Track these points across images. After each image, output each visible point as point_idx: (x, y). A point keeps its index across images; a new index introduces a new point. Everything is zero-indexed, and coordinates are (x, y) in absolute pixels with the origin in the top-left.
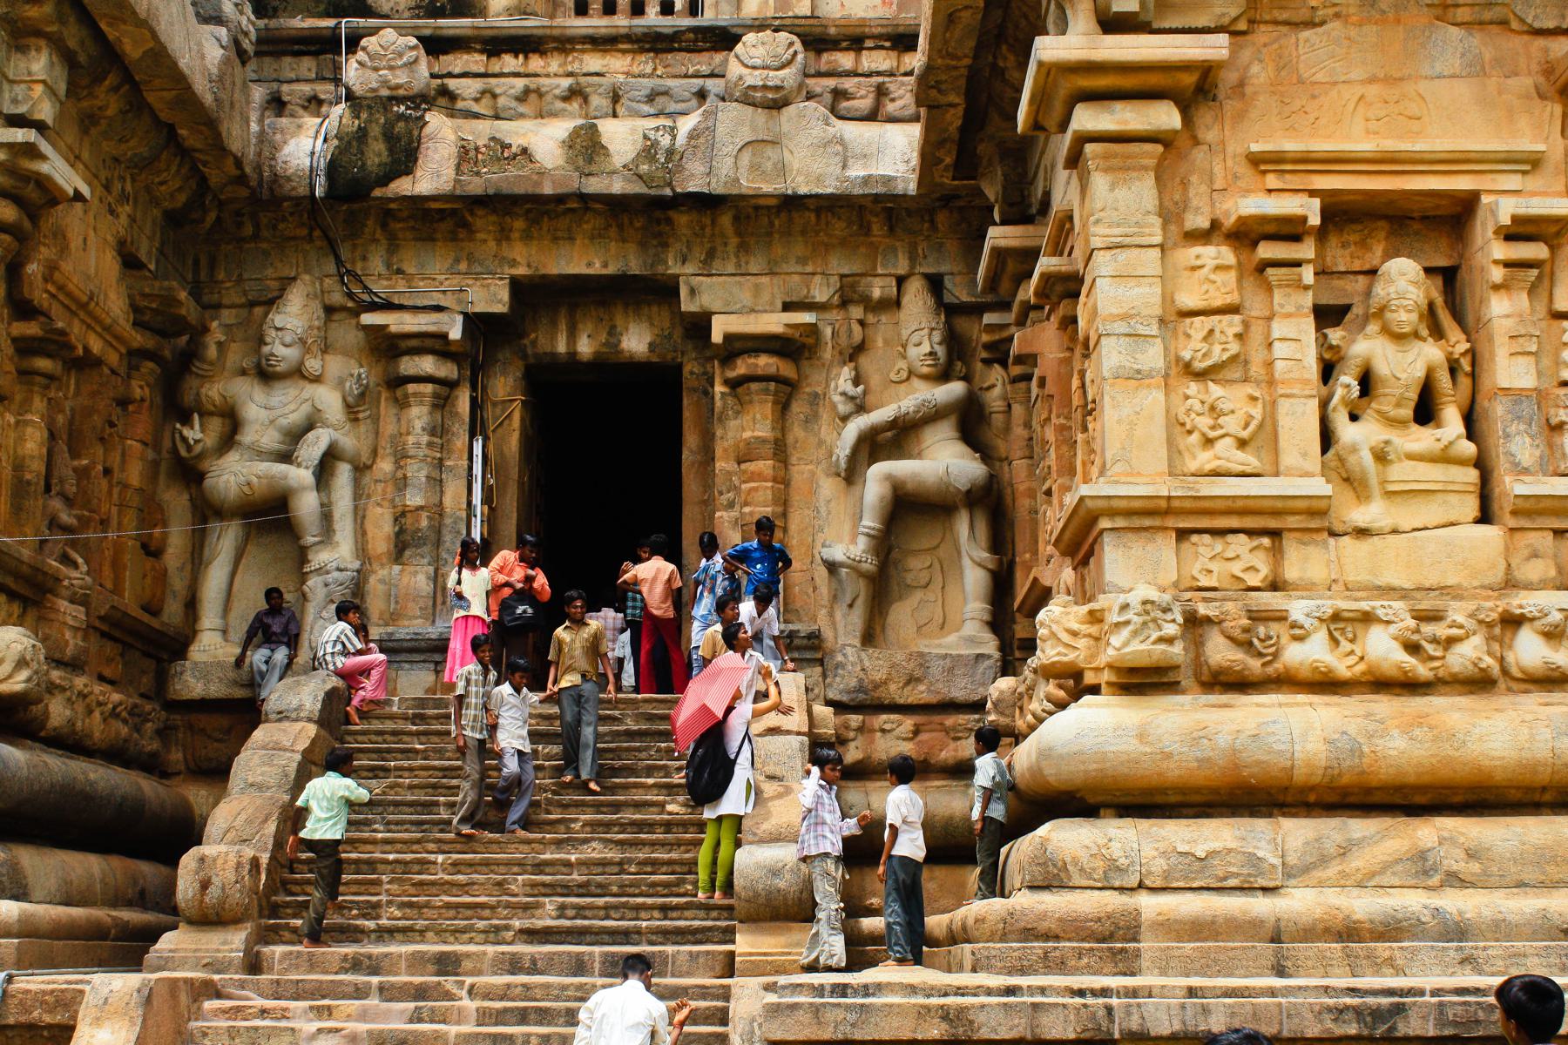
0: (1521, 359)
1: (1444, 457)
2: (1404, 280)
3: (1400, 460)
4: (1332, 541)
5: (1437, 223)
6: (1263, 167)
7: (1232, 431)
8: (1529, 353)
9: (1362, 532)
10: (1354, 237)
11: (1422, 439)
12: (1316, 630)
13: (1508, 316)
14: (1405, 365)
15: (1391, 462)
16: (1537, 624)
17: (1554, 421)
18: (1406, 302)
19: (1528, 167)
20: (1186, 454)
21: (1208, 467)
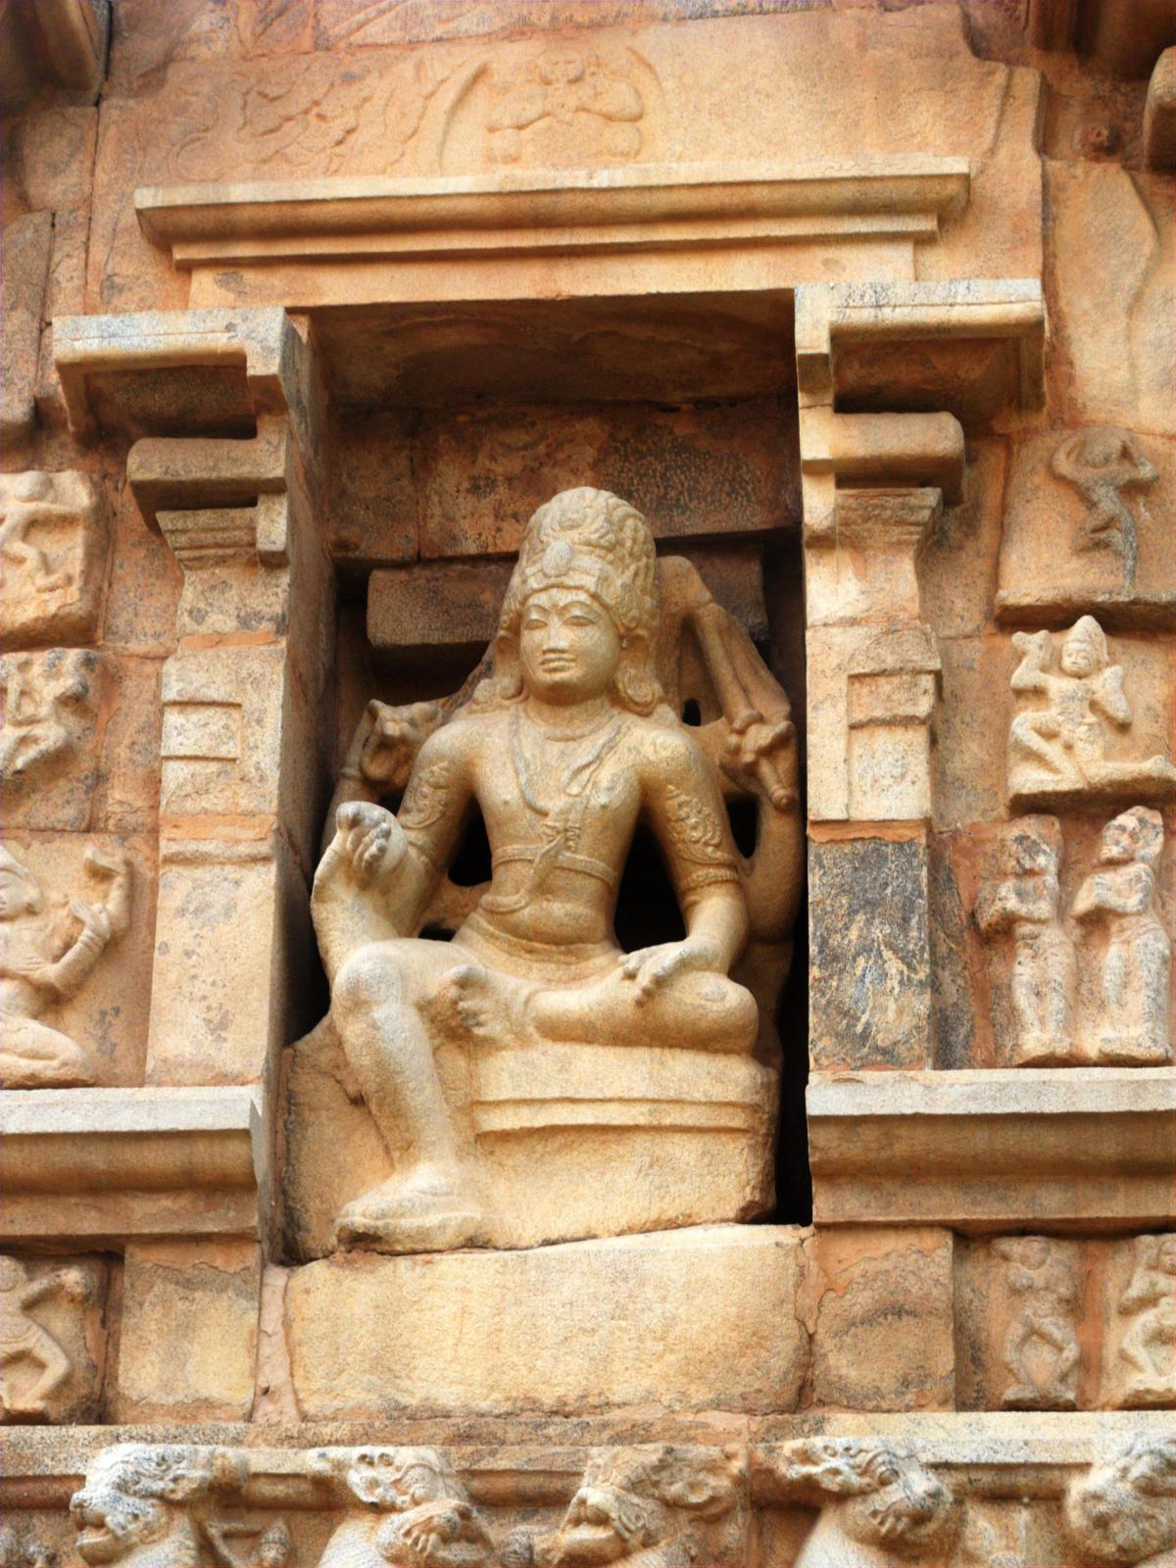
0: (883, 739)
1: (649, 1028)
2: (577, 548)
3: (523, 1040)
4: (277, 1277)
5: (683, 390)
6: (179, 254)
8: (908, 721)
9: (366, 1244)
11: (609, 982)
12: (151, 1534)
13: (853, 622)
15: (490, 1045)
16: (856, 1509)
17: (988, 916)
18: (563, 598)
19: (927, 224)
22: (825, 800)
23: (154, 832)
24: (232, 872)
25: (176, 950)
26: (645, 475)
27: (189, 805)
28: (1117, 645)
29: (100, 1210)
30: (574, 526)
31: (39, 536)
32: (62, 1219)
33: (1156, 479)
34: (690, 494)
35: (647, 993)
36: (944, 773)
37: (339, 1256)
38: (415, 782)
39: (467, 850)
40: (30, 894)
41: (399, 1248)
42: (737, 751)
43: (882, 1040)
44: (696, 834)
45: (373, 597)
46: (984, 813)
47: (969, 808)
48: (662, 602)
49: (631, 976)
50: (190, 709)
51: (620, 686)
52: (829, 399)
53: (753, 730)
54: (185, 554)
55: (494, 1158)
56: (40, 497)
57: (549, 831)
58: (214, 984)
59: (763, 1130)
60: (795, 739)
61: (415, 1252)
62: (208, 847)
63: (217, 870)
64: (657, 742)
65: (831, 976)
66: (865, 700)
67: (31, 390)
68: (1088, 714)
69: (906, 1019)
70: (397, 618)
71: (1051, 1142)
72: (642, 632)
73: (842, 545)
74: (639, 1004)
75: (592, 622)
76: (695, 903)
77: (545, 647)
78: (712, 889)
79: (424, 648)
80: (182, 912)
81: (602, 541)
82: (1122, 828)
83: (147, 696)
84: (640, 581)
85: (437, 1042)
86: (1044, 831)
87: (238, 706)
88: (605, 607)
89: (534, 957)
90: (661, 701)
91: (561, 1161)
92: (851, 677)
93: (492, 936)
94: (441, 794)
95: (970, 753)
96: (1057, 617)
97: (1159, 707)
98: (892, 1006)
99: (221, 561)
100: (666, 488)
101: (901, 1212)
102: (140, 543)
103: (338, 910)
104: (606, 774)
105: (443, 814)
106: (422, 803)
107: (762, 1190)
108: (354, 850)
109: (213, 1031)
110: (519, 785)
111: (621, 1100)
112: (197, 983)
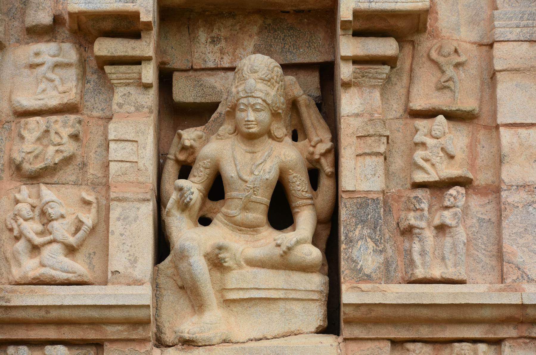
0: (368, 160)
1: (284, 263)
3: (240, 266)
7: (59, 237)
8: (378, 154)
13: (357, 115)
14: (254, 165)
20: (12, 262)
21: (32, 274)
22: (348, 181)
23: (107, 186)
24: (137, 205)
25: (117, 233)
26: (277, 39)
27: (120, 179)
28: (451, 124)
29: (95, 330)
31: (57, 70)
32: (82, 333)
33: (466, 61)
34: (293, 47)
35: (285, 252)
36: (388, 171)
37: (179, 347)
39: (216, 190)
40: (63, 211)
41: (200, 344)
42: (312, 154)
43: (367, 271)
44: (299, 188)
45: (174, 82)
46: (402, 186)
47: (397, 184)
50: (118, 142)
51: (272, 132)
52: (351, 32)
53: (319, 145)
54: (115, 82)
55: (229, 308)
56: (58, 55)
57: (247, 188)
58: (131, 246)
59: (324, 300)
60: (335, 152)
61: (205, 346)
62: (128, 195)
63: (131, 203)
65: (349, 248)
66: (362, 145)
67: (52, 12)
68: (441, 153)
69: (375, 264)
70: (184, 91)
71: (426, 313)
72: (280, 111)
73: (354, 85)
75: (263, 110)
76: (298, 212)
77: (246, 119)
78: (305, 207)
79: (194, 103)
80: (118, 219)
81: (266, 78)
82: (451, 195)
83: (101, 133)
85: (210, 267)
86: (424, 195)
87: (137, 141)
88: (268, 104)
89: (241, 232)
90: (286, 135)
91: (253, 310)
92: (357, 137)
93: (226, 224)
95: (398, 163)
96: (430, 114)
97: (465, 147)
98: (370, 259)
99: (128, 85)
100: (285, 44)
101: (373, 335)
102: (95, 72)
103: (175, 220)
104: (267, 166)
105: (208, 178)
106: (200, 174)
107: (323, 321)
108: (181, 199)
109: (131, 264)
110: (237, 170)
111: (275, 289)
112: (125, 246)
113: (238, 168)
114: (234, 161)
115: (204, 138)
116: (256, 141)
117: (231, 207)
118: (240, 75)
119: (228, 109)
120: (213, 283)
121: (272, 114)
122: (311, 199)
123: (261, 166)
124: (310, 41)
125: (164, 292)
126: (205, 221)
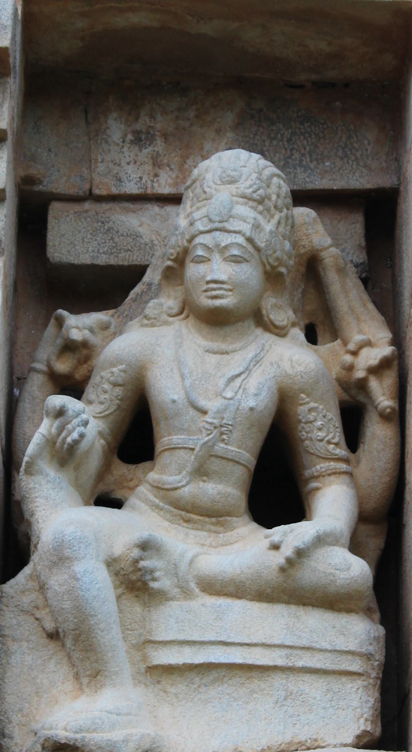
10: (161, 123)
18: (225, 239)
26: (275, 139)
30: (233, 182)
34: (311, 156)
35: (289, 561)
38: (95, 379)
39: (136, 436)
42: (350, 368)
44: (321, 434)
45: (52, 222)
48: (295, 245)
49: (276, 547)
51: (264, 312)
53: (365, 352)
55: (159, 686)
57: (207, 426)
59: (374, 675)
64: (292, 358)
70: (72, 241)
72: (283, 270)
74: (282, 570)
75: (247, 261)
76: (317, 489)
77: (208, 278)
78: (332, 478)
79: (93, 267)
81: (255, 195)
84: (281, 229)
85: (120, 591)
88: (258, 249)
89: (190, 526)
90: (294, 325)
91: (213, 692)
93: (157, 507)
94: (118, 391)
100: (291, 150)
105: (119, 406)
106: (103, 397)
107: (372, 722)
108: (59, 435)
110: (184, 387)
113: (188, 383)
114: (180, 369)
115: (112, 329)
116: (228, 329)
117: (169, 470)
118: (198, 190)
119: (169, 263)
120: (124, 628)
121: (266, 273)
122: (346, 461)
123: (239, 381)
124: (346, 146)
125: (13, 647)
126: (108, 500)
